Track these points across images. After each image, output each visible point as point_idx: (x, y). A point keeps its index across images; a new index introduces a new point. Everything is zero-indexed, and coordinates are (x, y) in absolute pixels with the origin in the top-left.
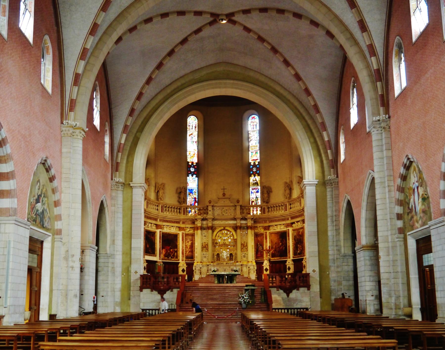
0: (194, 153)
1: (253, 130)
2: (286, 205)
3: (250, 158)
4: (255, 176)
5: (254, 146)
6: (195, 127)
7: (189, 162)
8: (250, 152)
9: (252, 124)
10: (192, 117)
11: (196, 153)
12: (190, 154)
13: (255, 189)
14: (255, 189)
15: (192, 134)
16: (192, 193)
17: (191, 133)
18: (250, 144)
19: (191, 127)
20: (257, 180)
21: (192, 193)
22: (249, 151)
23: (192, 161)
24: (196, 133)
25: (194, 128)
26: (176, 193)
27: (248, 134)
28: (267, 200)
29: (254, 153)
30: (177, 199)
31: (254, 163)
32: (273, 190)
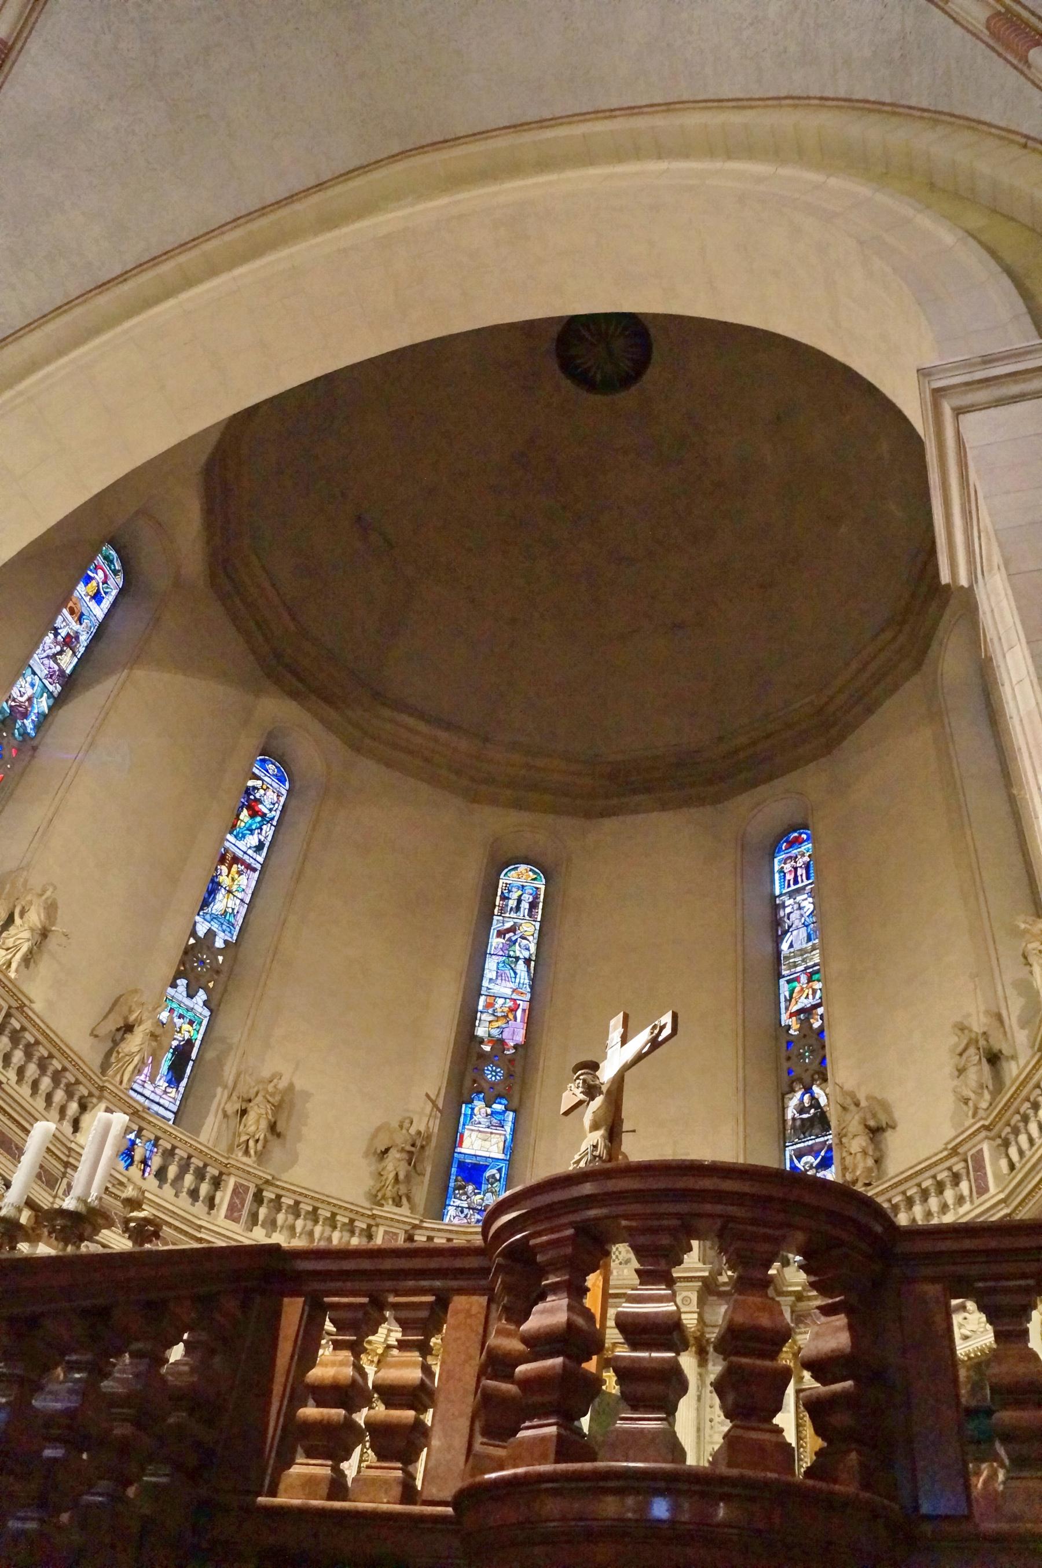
0: (510, 1004)
1: (793, 887)
2: (979, 1160)
3: (783, 1005)
4: (808, 1090)
5: (802, 952)
6: (533, 905)
7: (482, 1041)
8: (782, 982)
9: (787, 867)
10: (523, 868)
11: (524, 1005)
12: (489, 1005)
13: (810, 1151)
14: (810, 1151)
15: (513, 930)
16: (478, 1185)
17: (508, 925)
18: (785, 946)
19: (512, 903)
20: (823, 1101)
21: (478, 1185)
22: (780, 976)
23: (495, 1032)
24: (530, 928)
25: (525, 905)
26: (366, 1155)
27: (776, 908)
28: (870, 1170)
29: (804, 979)
30: (369, 1183)
31: (805, 1024)
32: (897, 1115)
